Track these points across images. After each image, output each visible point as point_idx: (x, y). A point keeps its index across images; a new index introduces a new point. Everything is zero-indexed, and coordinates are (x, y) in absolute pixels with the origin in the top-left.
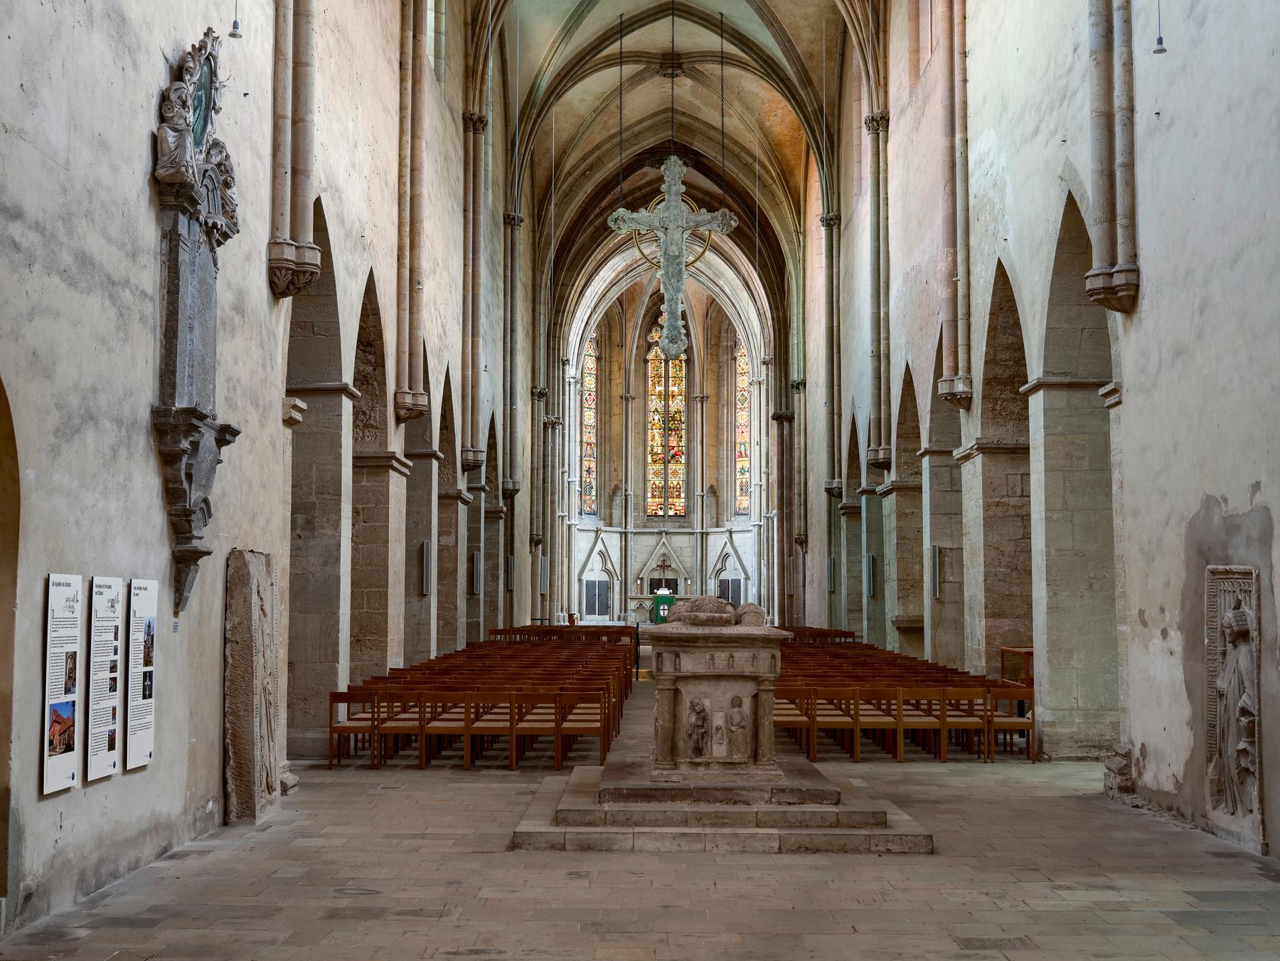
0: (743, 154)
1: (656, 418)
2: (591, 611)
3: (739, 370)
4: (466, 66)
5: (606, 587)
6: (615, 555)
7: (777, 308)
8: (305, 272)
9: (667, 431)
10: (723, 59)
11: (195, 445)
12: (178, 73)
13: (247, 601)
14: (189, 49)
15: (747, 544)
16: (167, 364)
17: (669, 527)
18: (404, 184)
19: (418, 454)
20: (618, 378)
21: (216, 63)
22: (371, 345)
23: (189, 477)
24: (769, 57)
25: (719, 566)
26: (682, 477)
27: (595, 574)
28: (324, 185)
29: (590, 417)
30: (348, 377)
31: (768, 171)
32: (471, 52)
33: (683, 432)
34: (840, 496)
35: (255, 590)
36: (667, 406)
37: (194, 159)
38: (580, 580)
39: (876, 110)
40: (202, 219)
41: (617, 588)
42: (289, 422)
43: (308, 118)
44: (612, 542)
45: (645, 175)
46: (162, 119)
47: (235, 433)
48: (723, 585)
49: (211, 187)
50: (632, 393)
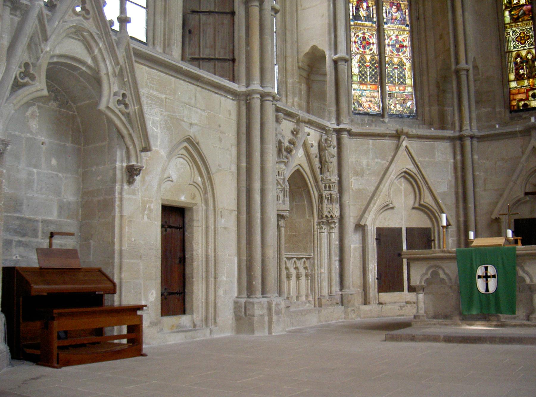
38: (360, 228)
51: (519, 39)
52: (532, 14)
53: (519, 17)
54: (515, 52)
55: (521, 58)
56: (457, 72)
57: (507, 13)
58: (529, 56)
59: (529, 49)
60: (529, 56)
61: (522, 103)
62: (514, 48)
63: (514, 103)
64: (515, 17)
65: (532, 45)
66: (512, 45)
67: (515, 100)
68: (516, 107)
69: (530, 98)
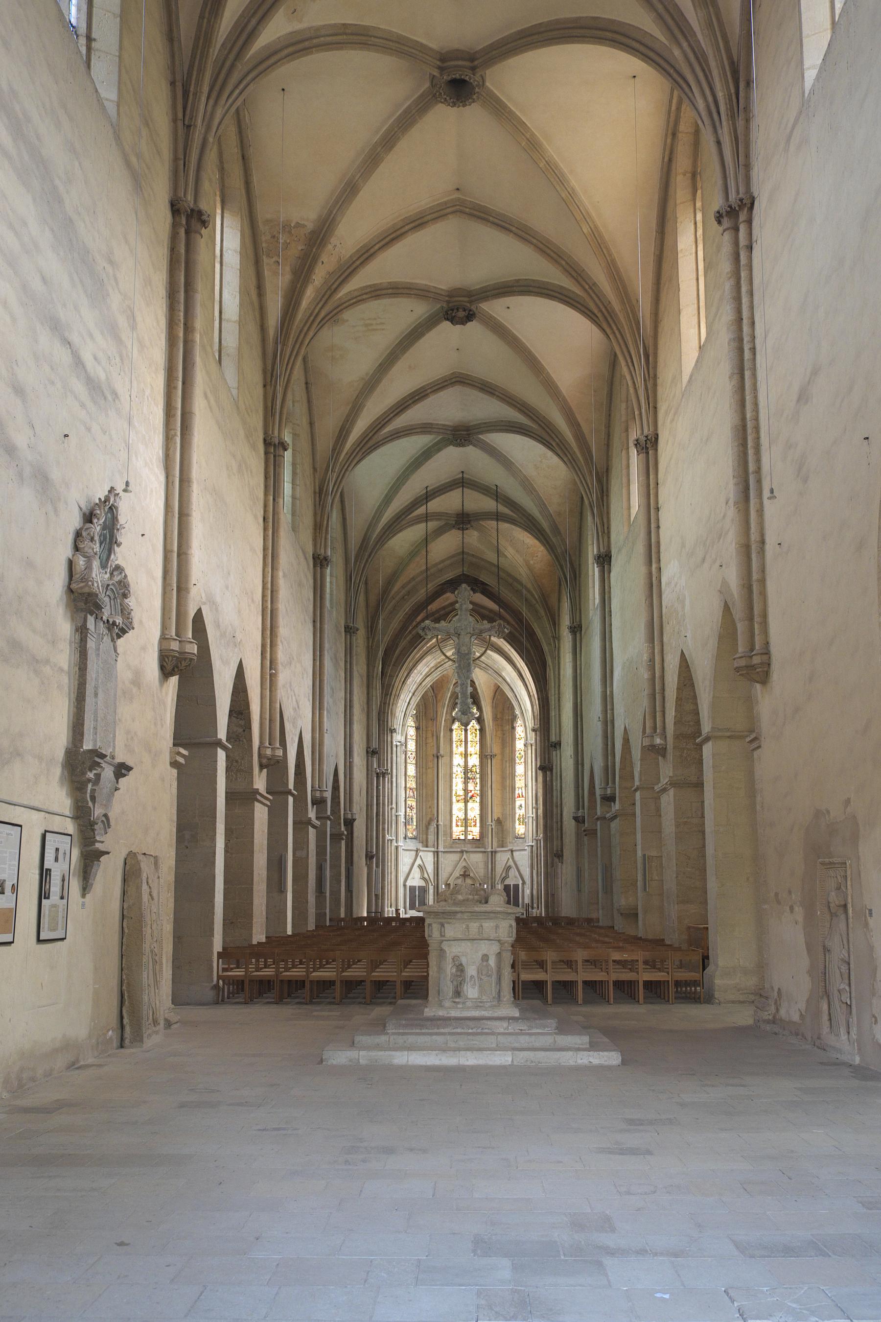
0: (515, 584)
2: (412, 907)
3: (517, 736)
4: (315, 521)
5: (423, 890)
6: (430, 868)
7: (541, 691)
8: (185, 659)
9: (466, 780)
10: (498, 517)
11: (98, 776)
12: (89, 517)
13: (139, 888)
14: (97, 502)
15: (523, 859)
16: (78, 719)
17: (468, 848)
18: (266, 601)
19: (277, 790)
20: (431, 742)
21: (117, 511)
22: (242, 714)
23: (93, 799)
24: (530, 515)
25: (504, 875)
27: (415, 881)
28: (204, 600)
29: (412, 770)
30: (222, 734)
31: (532, 595)
32: (319, 512)
33: (478, 781)
34: (584, 822)
35: (144, 881)
36: (466, 762)
37: (99, 577)
38: (405, 886)
39: (602, 550)
40: (105, 618)
41: (431, 891)
42: (174, 764)
43: (189, 552)
44: (428, 859)
45: (447, 599)
46: (76, 548)
47: (129, 769)
48: (507, 888)
49: (112, 597)
50: (442, 752)
56: (437, 826)
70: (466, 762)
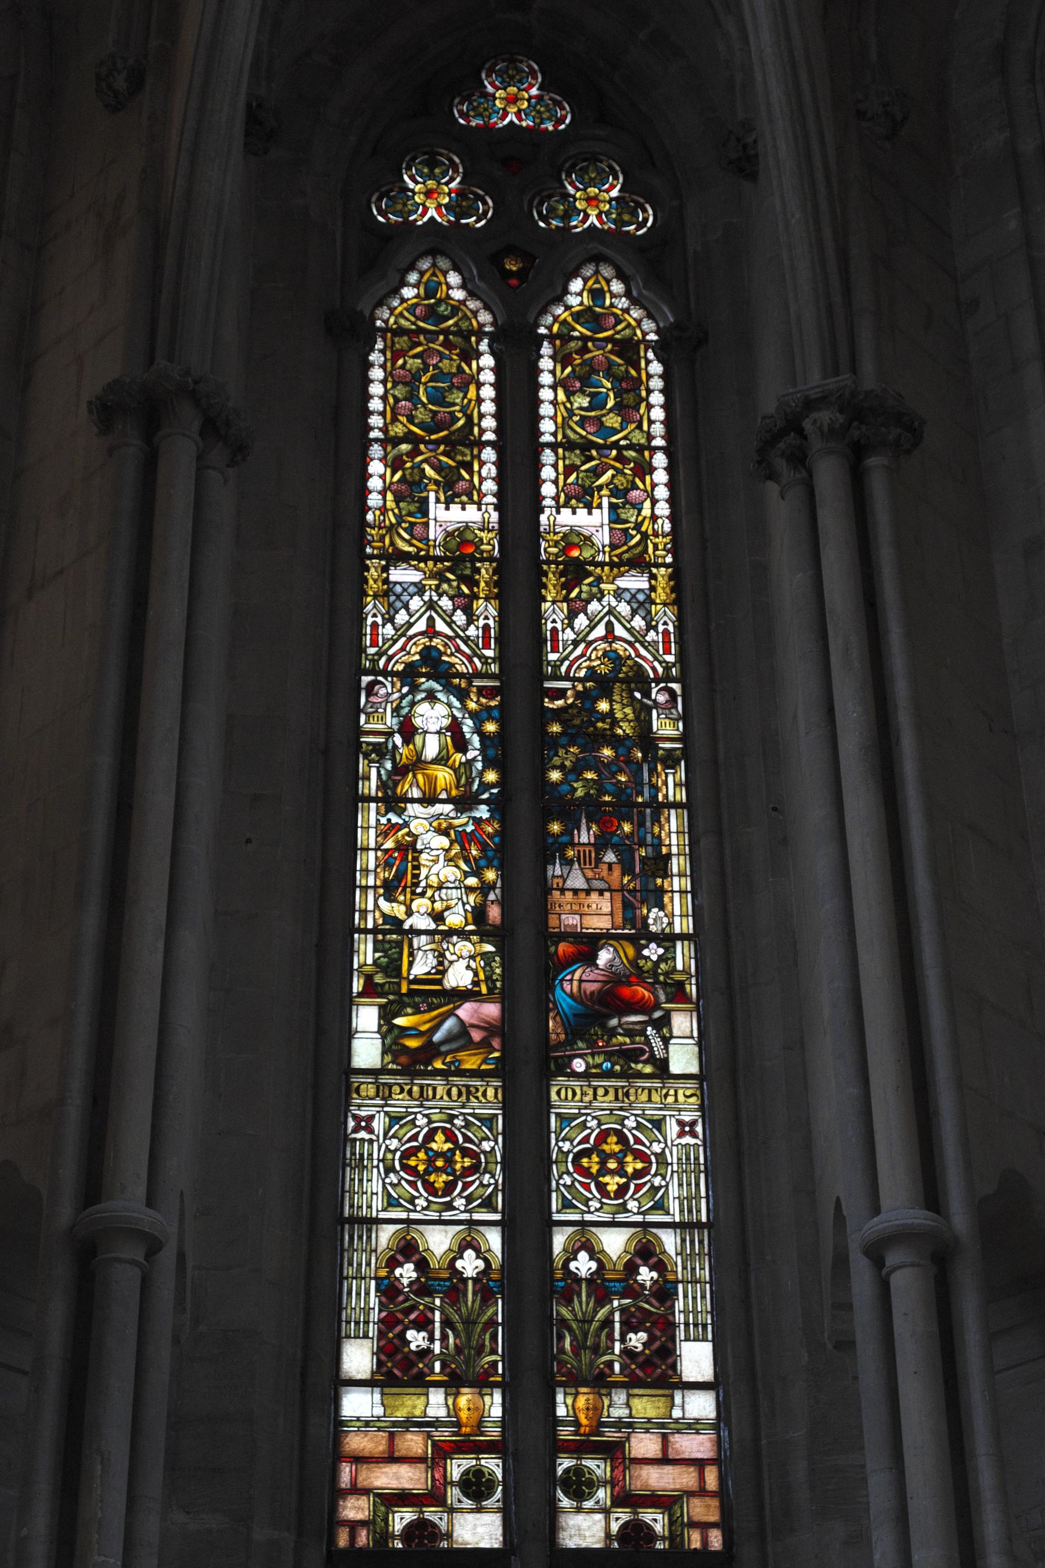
1: (431, 716)
26: (681, 1193)
36: (521, 639)
51: (419, 1162)
52: (503, 1050)
53: (430, 1051)
54: (392, 1228)
55: (422, 1265)
57: (366, 1018)
58: (470, 1265)
59: (471, 1223)
60: (470, 1265)
61: (401, 1519)
62: (391, 1203)
63: (355, 1509)
64: (413, 1043)
65: (488, 1204)
66: (376, 1186)
67: (366, 1491)
68: (363, 1538)
69: (454, 1494)
70: (521, 639)
